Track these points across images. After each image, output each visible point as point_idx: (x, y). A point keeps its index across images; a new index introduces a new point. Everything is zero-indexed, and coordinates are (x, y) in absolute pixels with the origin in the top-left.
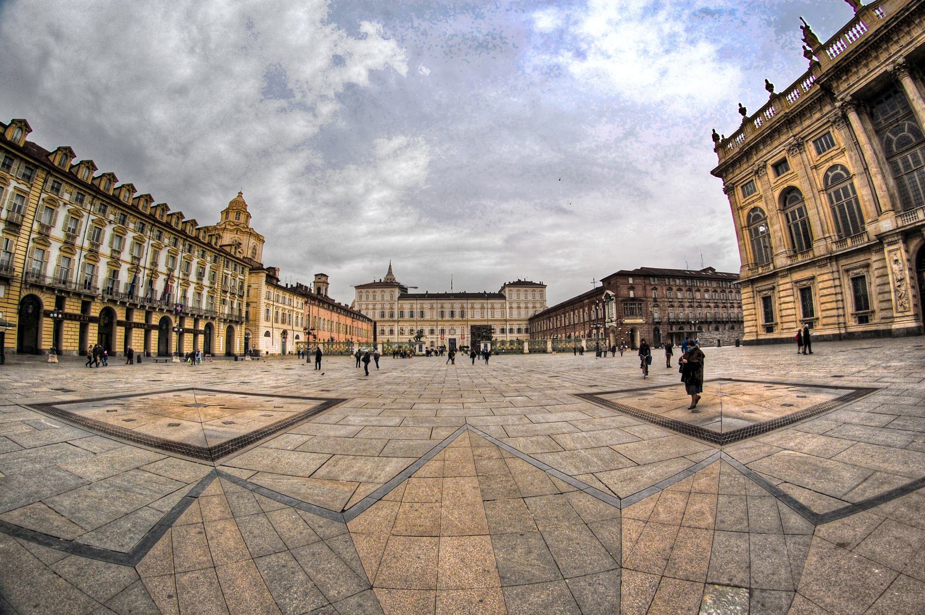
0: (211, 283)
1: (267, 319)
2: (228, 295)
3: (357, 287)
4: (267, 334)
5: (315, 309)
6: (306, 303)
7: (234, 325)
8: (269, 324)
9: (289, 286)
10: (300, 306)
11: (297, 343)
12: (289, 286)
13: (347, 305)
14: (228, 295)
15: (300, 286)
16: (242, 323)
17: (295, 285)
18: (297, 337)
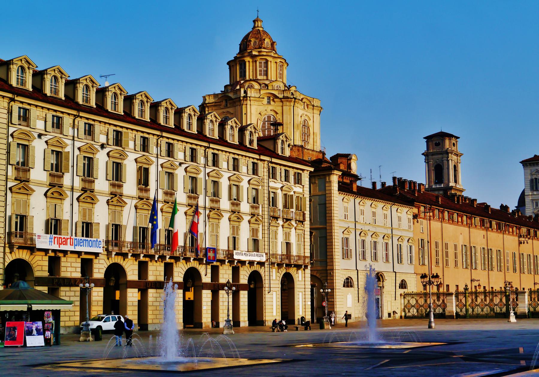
0: (252, 207)
1: (346, 255)
2: (280, 222)
3: (526, 163)
4: (348, 283)
5: (436, 225)
6: (415, 217)
7: (292, 271)
8: (350, 264)
9: (379, 187)
10: (405, 224)
11: (405, 296)
12: (379, 187)
13: (504, 208)
14: (280, 222)
15: (400, 183)
16: (306, 267)
17: (390, 183)
18: (403, 285)
